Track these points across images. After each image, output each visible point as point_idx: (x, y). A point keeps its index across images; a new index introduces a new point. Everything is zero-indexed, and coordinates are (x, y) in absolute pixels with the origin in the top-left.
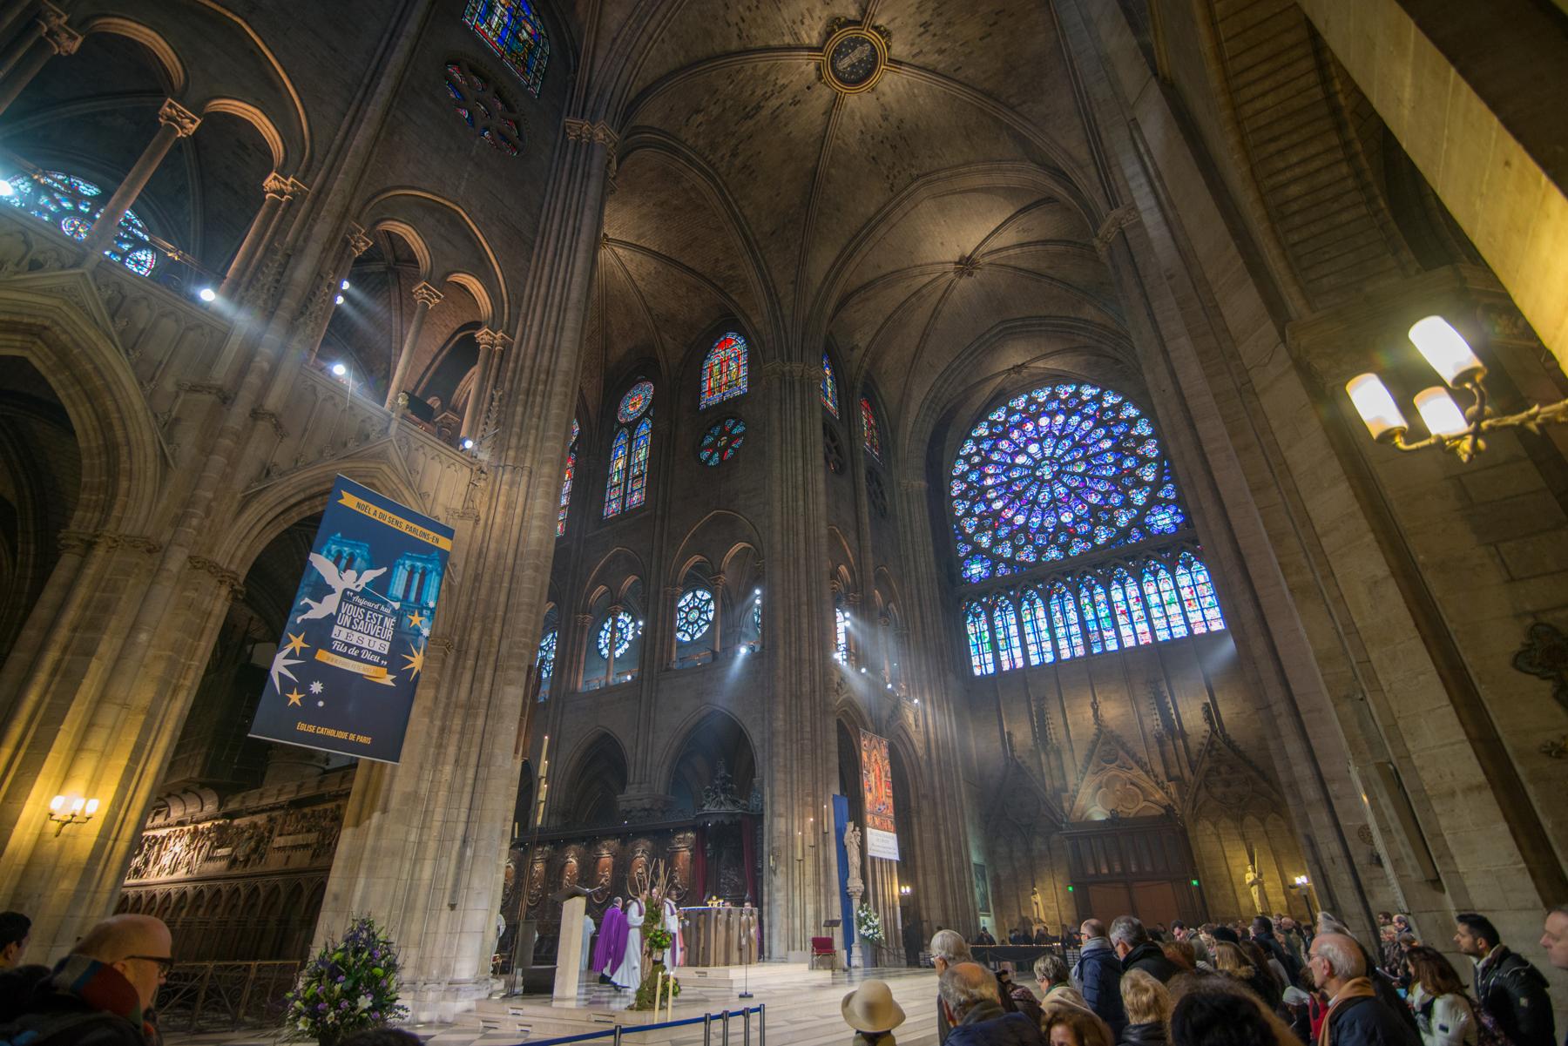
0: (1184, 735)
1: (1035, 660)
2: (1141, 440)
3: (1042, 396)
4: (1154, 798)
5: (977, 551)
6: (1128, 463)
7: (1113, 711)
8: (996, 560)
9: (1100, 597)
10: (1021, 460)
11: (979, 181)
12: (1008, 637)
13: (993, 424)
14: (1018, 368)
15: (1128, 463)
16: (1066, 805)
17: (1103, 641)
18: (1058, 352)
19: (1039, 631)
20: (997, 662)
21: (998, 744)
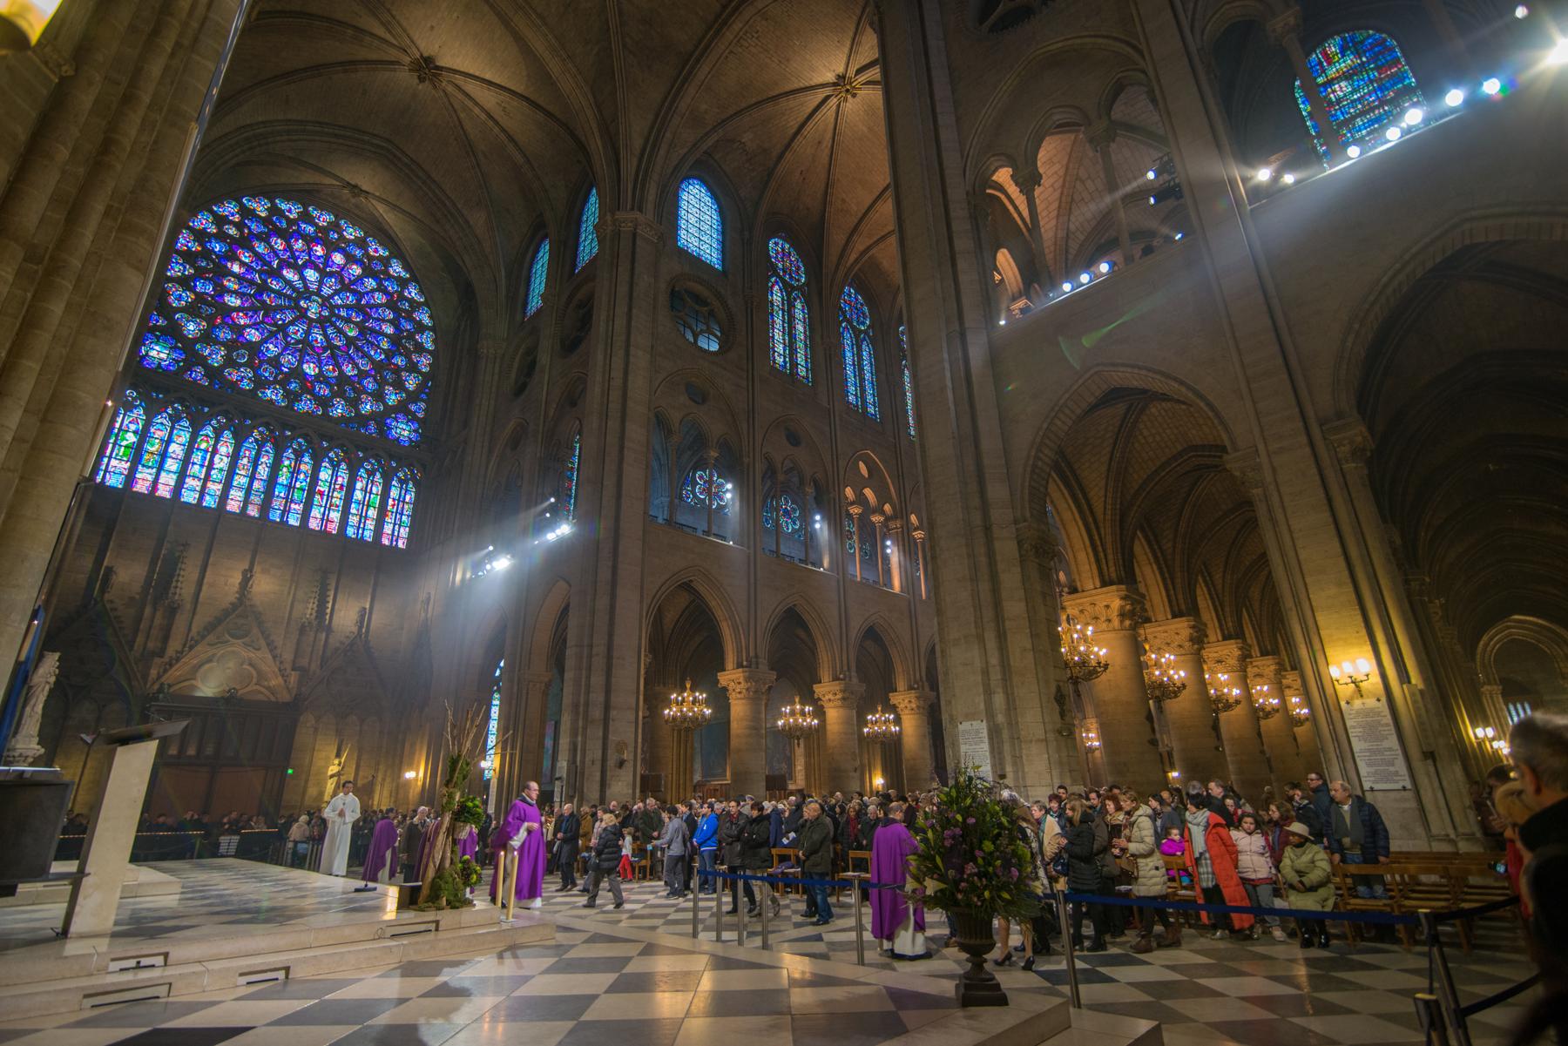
0: (329, 630)
1: (189, 497)
2: (420, 348)
3: (351, 233)
4: (276, 683)
5: (172, 334)
6: (399, 361)
7: (265, 585)
8: (193, 358)
9: (306, 467)
10: (289, 274)
11: (539, 45)
12: (164, 455)
13: (274, 210)
14: (356, 190)
15: (399, 361)
16: (154, 673)
17: (286, 511)
18: (414, 218)
19: (211, 467)
20: (131, 478)
21: (82, 579)
